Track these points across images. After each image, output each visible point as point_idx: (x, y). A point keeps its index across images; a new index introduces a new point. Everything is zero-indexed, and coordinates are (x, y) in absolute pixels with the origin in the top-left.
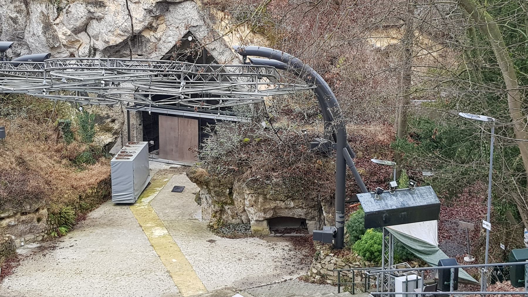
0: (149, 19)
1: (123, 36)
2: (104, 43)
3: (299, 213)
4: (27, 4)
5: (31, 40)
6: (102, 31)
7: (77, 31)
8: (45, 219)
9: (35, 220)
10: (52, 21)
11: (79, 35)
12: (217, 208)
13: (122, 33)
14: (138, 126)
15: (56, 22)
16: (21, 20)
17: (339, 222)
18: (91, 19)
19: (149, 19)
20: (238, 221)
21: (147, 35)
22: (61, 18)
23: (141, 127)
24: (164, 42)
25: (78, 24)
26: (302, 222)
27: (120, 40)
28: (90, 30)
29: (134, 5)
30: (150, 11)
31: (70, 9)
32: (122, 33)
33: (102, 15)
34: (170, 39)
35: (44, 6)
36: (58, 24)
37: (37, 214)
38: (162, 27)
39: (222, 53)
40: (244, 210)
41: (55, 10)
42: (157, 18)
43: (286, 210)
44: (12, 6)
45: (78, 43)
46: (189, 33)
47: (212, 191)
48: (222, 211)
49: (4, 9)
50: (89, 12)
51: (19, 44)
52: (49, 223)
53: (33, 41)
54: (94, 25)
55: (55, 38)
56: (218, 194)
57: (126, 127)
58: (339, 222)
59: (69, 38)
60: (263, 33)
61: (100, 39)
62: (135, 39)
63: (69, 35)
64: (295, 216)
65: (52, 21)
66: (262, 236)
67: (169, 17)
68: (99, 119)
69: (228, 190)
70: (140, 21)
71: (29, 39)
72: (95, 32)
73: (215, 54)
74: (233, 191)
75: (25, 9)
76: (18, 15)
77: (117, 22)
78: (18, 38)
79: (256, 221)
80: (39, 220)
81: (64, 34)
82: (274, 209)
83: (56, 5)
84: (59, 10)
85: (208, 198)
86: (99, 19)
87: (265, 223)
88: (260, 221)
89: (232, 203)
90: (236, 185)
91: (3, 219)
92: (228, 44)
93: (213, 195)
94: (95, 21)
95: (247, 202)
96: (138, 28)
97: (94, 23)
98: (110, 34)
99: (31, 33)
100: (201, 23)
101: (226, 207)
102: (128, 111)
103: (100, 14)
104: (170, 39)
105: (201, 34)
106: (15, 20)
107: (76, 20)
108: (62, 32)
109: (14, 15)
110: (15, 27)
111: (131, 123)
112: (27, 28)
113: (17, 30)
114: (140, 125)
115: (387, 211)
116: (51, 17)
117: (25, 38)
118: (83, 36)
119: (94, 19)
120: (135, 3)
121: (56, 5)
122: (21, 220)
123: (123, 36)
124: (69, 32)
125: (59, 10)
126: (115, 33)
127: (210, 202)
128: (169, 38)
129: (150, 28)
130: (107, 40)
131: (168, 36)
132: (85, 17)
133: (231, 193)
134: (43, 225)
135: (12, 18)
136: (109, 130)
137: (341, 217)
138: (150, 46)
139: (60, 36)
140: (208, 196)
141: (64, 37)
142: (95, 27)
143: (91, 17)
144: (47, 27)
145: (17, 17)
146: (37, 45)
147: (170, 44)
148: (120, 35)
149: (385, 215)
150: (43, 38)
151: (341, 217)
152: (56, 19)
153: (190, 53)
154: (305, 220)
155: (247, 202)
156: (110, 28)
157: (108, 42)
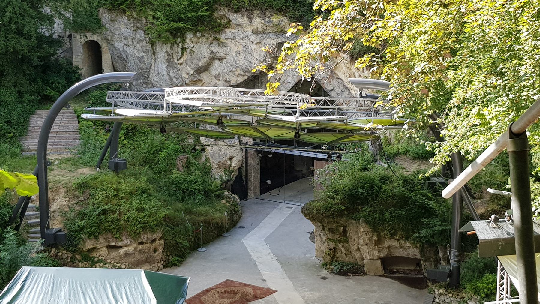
1: (243, 76)
2: (225, 83)
5: (155, 79)
6: (224, 71)
7: (200, 71)
8: (160, 250)
9: (152, 250)
10: (176, 61)
11: (201, 75)
13: (243, 73)
14: (255, 165)
15: (179, 62)
17: (455, 261)
18: (214, 59)
22: (185, 58)
23: (259, 167)
24: (284, 82)
25: (200, 64)
29: (255, 45)
31: (193, 49)
32: (243, 73)
33: (225, 56)
35: (169, 46)
36: (181, 64)
37: (154, 244)
39: (340, 94)
40: (359, 249)
41: (180, 50)
43: (401, 250)
44: (138, 46)
45: (200, 82)
47: (326, 228)
49: (131, 49)
50: (212, 52)
51: (144, 83)
52: (165, 254)
53: (158, 80)
54: (216, 65)
57: (244, 165)
58: (455, 261)
59: (192, 77)
61: (221, 78)
63: (192, 75)
64: (410, 256)
65: (176, 61)
69: (342, 228)
70: (260, 61)
71: (154, 77)
72: (217, 72)
74: (347, 229)
75: (150, 48)
76: (144, 54)
77: (239, 62)
79: (370, 259)
80: (155, 251)
81: (187, 74)
82: (389, 247)
83: (180, 45)
84: (183, 49)
85: (322, 235)
86: (221, 59)
87: (379, 262)
88: (374, 260)
91: (121, 247)
92: (346, 84)
93: (328, 232)
94: (217, 61)
95: (361, 241)
97: (216, 63)
98: (231, 74)
99: (156, 72)
101: (340, 245)
102: (246, 150)
103: (222, 54)
104: (290, 79)
106: (141, 59)
107: (199, 60)
110: (141, 65)
111: (249, 162)
112: (152, 67)
113: (144, 69)
114: (258, 164)
115: (504, 239)
116: (175, 57)
117: (150, 77)
119: (216, 59)
120: (257, 43)
121: (180, 45)
122: (138, 249)
123: (243, 76)
124: (192, 72)
125: (183, 49)
126: (237, 73)
127: (324, 239)
128: (289, 78)
130: (228, 80)
132: (207, 58)
134: (159, 255)
135: (138, 58)
137: (456, 256)
139: (184, 75)
140: (322, 234)
141: (187, 77)
143: (214, 57)
145: (143, 57)
146: (161, 83)
147: (289, 84)
148: (241, 75)
149: (500, 243)
151: (456, 256)
152: (180, 58)
154: (420, 260)
156: (231, 68)
157: (229, 82)
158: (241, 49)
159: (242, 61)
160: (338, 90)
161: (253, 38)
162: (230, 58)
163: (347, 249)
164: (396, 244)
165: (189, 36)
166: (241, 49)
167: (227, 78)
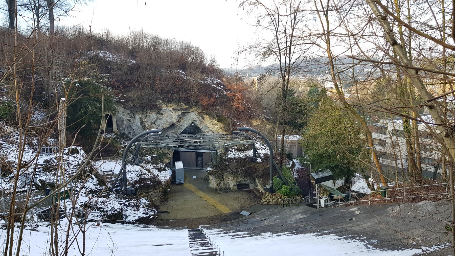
0: (178, 118)
3: (248, 182)
4: (134, 114)
7: (152, 124)
12: (218, 182)
16: (132, 120)
19: (178, 118)
20: (225, 186)
21: (176, 124)
25: (153, 121)
26: (247, 185)
27: (168, 126)
28: (156, 123)
30: (179, 116)
34: (185, 125)
38: (183, 121)
39: (205, 129)
42: (181, 118)
46: (193, 123)
48: (220, 183)
55: (145, 126)
56: (219, 178)
60: (221, 122)
62: (172, 126)
66: (235, 191)
67: (185, 117)
68: (165, 154)
71: (134, 127)
73: (202, 130)
78: (130, 127)
84: (146, 116)
86: (160, 119)
89: (224, 180)
90: (225, 174)
96: (175, 121)
100: (197, 119)
104: (185, 125)
105: (197, 123)
106: (130, 121)
108: (147, 124)
109: (129, 119)
118: (153, 125)
125: (146, 116)
129: (178, 121)
131: (185, 124)
133: (223, 177)
136: (168, 158)
138: (178, 128)
139: (147, 125)
142: (159, 122)
144: (142, 123)
150: (140, 126)
153: (194, 129)
155: (230, 180)
158: (168, 115)
159: (169, 119)
160: (204, 128)
161: (172, 111)
162: (164, 119)
163: (224, 183)
164: (242, 179)
165: (149, 111)
166: (168, 115)
167: (163, 125)
